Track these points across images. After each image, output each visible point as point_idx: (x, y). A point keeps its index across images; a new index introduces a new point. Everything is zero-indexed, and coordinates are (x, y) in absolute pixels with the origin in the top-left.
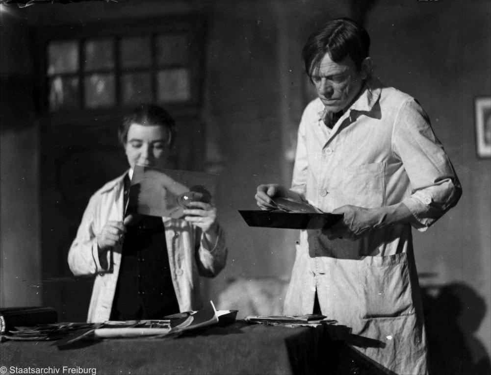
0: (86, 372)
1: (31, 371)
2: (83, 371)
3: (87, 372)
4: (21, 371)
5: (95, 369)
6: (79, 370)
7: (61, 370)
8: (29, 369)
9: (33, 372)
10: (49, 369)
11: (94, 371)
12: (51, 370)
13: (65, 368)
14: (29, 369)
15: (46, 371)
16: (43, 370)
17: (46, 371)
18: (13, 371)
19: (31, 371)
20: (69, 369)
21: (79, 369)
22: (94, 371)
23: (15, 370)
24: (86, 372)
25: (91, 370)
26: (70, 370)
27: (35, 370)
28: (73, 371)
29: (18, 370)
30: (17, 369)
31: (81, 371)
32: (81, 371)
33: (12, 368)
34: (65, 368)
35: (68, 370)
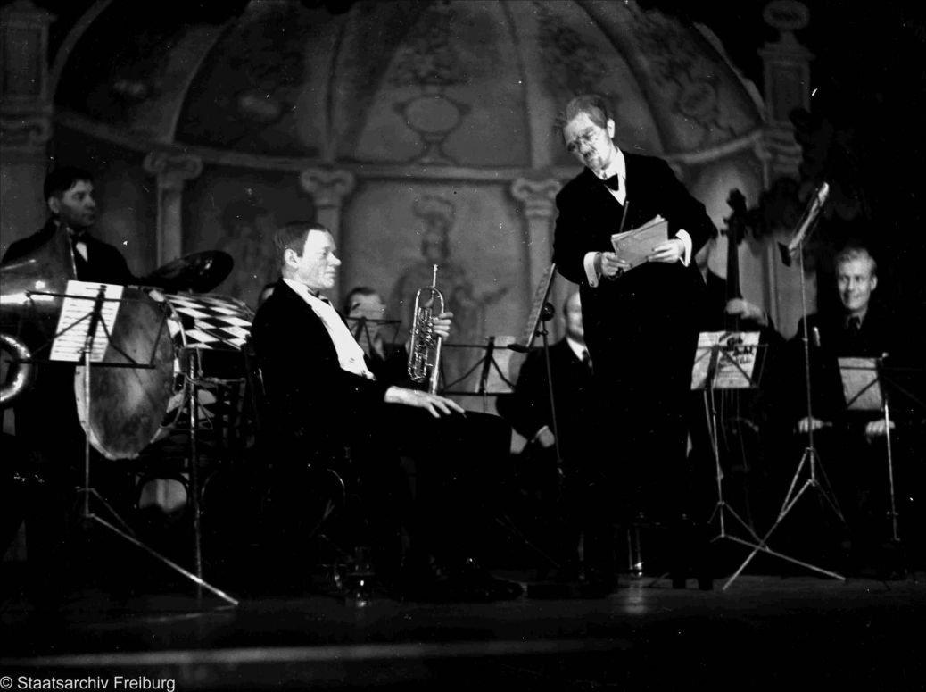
0: (156, 685)
1: (56, 684)
2: (152, 684)
3: (159, 687)
4: (39, 685)
5: (173, 681)
7: (111, 684)
8: (53, 680)
9: (60, 686)
10: (90, 681)
12: (92, 683)
13: (118, 680)
14: (53, 680)
15: (84, 684)
16: (78, 683)
18: (23, 685)
19: (56, 684)
20: (126, 682)
21: (144, 681)
22: (171, 684)
24: (156, 685)
25: (165, 683)
26: (128, 683)
27: (64, 684)
29: (33, 684)
30: (30, 680)
31: (147, 684)
32: (147, 684)
33: (22, 680)
34: (118, 680)
35: (124, 682)
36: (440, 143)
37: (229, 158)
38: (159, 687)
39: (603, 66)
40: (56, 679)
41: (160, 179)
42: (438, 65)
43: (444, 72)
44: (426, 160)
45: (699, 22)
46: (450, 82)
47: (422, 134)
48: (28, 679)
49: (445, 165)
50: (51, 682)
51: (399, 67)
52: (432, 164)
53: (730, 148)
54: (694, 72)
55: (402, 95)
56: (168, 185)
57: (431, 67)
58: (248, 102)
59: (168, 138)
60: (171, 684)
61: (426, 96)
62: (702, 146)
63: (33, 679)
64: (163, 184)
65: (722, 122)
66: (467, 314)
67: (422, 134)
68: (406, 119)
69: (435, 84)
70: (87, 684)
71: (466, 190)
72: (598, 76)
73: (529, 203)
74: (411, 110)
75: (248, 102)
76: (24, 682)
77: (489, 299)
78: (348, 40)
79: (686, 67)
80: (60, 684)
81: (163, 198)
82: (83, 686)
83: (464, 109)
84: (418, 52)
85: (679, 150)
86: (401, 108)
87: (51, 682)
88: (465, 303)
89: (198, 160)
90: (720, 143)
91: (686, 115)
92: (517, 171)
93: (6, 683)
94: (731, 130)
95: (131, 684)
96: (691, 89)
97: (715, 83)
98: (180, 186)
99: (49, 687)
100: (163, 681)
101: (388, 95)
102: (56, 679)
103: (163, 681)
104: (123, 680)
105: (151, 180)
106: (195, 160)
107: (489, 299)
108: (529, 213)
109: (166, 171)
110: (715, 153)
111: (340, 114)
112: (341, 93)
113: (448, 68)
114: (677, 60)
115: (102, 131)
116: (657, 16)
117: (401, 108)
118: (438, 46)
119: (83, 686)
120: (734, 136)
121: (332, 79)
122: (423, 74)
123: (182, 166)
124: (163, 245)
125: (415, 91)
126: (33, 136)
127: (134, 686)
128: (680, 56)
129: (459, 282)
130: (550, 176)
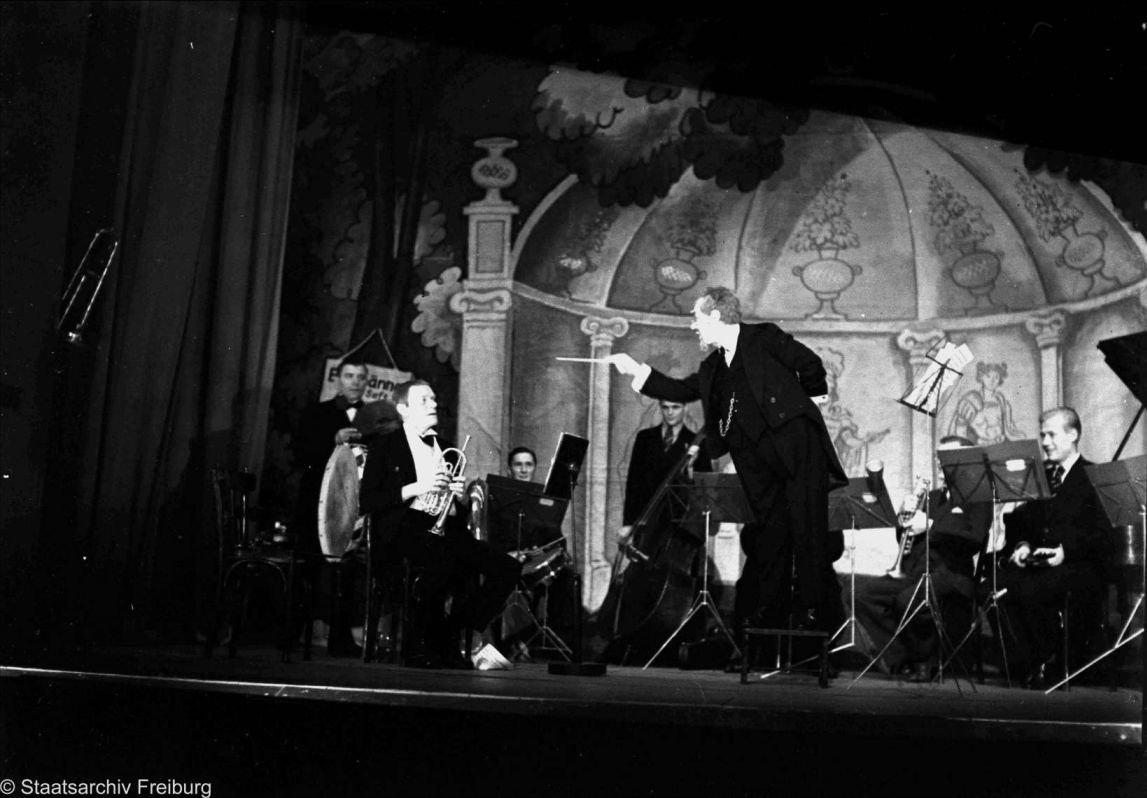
0: (188, 790)
2: (183, 788)
3: (191, 792)
4: (47, 789)
5: (209, 785)
6: (173, 787)
7: (134, 787)
8: (64, 784)
9: (73, 791)
11: (206, 790)
13: (143, 783)
14: (64, 784)
15: (101, 789)
16: (94, 788)
17: (101, 789)
18: (28, 790)
20: (152, 785)
22: (206, 789)
23: (34, 787)
24: (188, 790)
25: (199, 787)
26: (155, 788)
27: (78, 788)
28: (160, 788)
30: (36, 784)
31: (177, 789)
32: (177, 789)
33: (27, 783)
34: (143, 783)
36: (832, 300)
37: (649, 319)
38: (191, 792)
39: (991, 227)
40: (68, 783)
41: (592, 338)
42: (833, 232)
43: (840, 239)
44: (821, 315)
45: (1086, 179)
46: (845, 247)
47: (816, 293)
48: (34, 782)
49: (837, 320)
50: (62, 787)
51: (799, 236)
52: (827, 319)
53: (1118, 296)
54: (1080, 228)
55: (799, 260)
56: (600, 343)
57: (829, 236)
58: (667, 271)
59: (601, 305)
60: (206, 789)
61: (821, 259)
62: (1086, 297)
63: (40, 783)
64: (594, 344)
65: (1107, 272)
66: (852, 451)
67: (816, 293)
68: (803, 281)
69: (829, 248)
70: (105, 788)
71: (855, 341)
72: (984, 236)
73: (914, 353)
74: (805, 274)
75: (667, 271)
76: (29, 786)
77: (872, 438)
78: (756, 209)
79: (1073, 221)
80: (73, 789)
81: (596, 352)
82: (101, 791)
83: (855, 271)
84: (816, 221)
85: (1064, 301)
86: (799, 271)
87: (62, 787)
88: (850, 441)
89: (625, 321)
90: (1105, 292)
91: (1072, 268)
92: (904, 323)
93: (7, 787)
94: (1116, 280)
95: (158, 789)
96: (1076, 243)
97: (1101, 236)
98: (610, 344)
99: (59, 792)
100: (197, 786)
101: (788, 259)
102: (68, 783)
103: (197, 786)
104: (148, 784)
105: (586, 339)
106: (622, 321)
107: (872, 438)
108: (913, 361)
109: (598, 332)
110: (1101, 301)
111: (744, 275)
112: (747, 261)
113: (842, 234)
114: (1065, 217)
115: (550, 300)
116: (1044, 176)
117: (799, 271)
118: (835, 215)
119: (101, 791)
120: (1120, 286)
121: (740, 248)
122: (820, 241)
123: (611, 326)
124: (594, 392)
125: (815, 254)
126: (497, 304)
127: (161, 791)
128: (1067, 213)
129: (846, 423)
130: (935, 327)
